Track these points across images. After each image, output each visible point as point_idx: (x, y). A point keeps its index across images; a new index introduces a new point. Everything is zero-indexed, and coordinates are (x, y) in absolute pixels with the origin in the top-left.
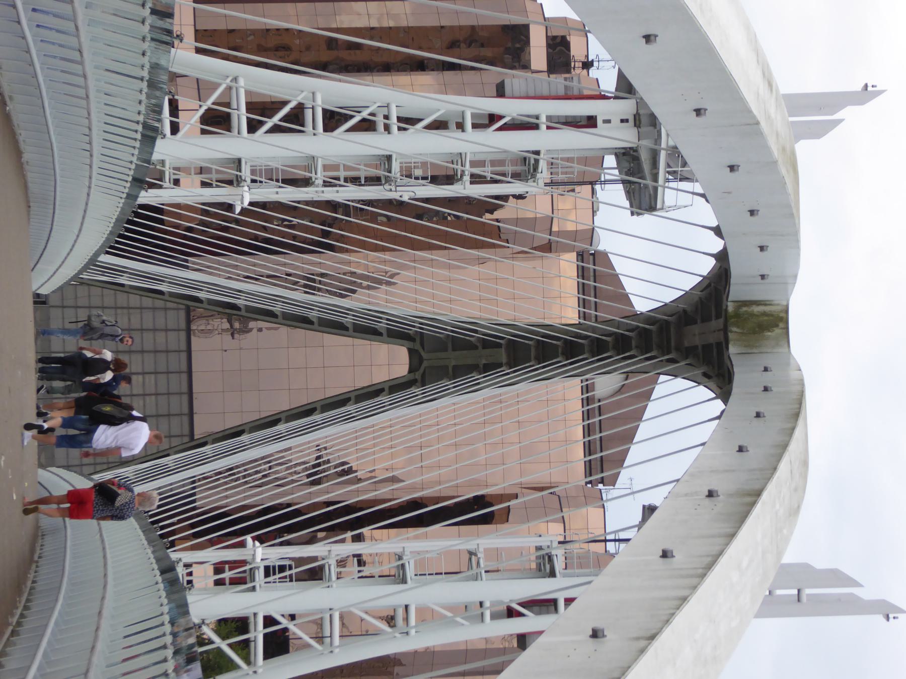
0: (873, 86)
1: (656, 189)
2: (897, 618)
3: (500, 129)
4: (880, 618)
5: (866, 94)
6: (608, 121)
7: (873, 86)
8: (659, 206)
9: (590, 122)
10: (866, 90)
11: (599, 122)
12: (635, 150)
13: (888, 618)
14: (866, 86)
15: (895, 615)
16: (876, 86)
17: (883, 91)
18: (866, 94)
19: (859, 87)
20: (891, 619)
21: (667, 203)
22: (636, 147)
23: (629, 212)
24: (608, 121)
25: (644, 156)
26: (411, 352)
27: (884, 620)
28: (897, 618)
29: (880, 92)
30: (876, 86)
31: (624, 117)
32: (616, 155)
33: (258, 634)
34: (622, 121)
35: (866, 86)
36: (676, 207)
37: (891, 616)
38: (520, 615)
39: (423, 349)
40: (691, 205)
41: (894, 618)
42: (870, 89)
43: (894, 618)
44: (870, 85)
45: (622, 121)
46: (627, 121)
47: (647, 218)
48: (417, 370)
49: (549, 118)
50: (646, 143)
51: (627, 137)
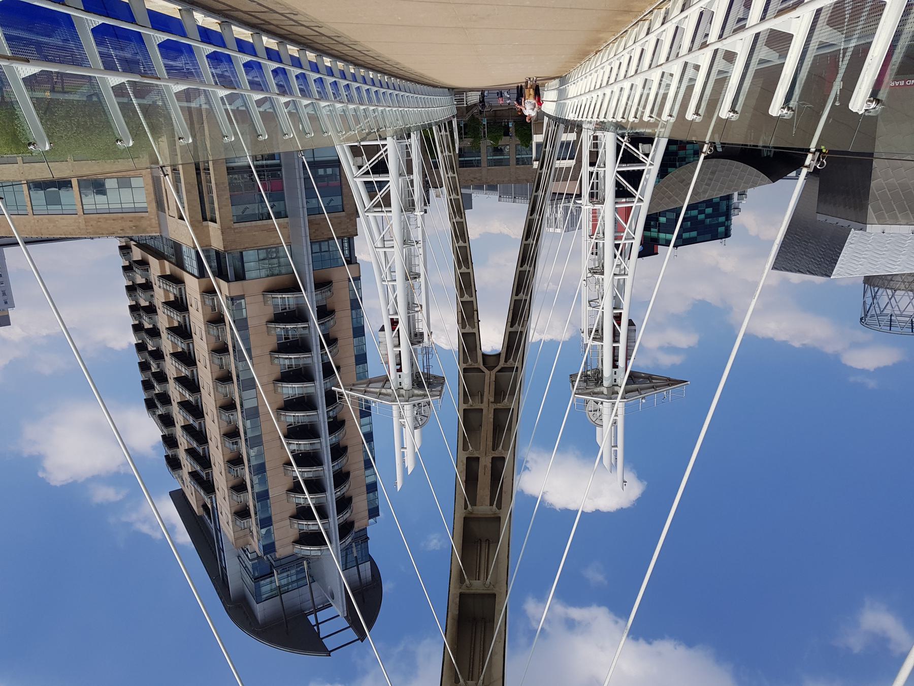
3: (614, 326)
6: (615, 374)
9: (615, 366)
11: (615, 370)
14: (626, 482)
24: (615, 374)
25: (598, 390)
38: (393, 330)
39: (499, 371)
42: (624, 483)
46: (615, 382)
48: (484, 364)
50: (605, 392)
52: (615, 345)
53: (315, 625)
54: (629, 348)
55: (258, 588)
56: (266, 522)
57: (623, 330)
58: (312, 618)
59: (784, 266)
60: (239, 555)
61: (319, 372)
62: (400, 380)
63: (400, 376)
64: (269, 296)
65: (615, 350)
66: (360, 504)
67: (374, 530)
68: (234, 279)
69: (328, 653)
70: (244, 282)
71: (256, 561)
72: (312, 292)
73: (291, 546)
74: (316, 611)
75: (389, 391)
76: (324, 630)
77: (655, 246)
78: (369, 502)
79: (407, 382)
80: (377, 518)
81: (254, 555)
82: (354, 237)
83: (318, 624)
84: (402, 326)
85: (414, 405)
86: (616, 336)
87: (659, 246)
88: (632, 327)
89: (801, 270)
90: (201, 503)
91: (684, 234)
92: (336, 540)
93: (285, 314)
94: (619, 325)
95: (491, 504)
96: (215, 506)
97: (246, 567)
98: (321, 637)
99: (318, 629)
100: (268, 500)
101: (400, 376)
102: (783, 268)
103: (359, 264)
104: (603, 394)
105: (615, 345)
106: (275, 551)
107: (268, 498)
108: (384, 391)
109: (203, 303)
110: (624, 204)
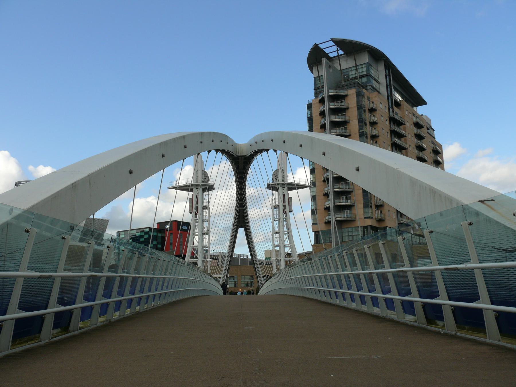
1: (209, 185)
3: (198, 212)
8: (213, 185)
12: (202, 189)
23: (213, 190)
26: (240, 227)
32: (203, 193)
33: (288, 259)
36: (213, 182)
38: (286, 212)
47: (215, 186)
49: (196, 204)
51: (200, 190)
52: (197, 205)
53: (339, 50)
54: (192, 203)
55: (368, 70)
56: (360, 107)
57: (194, 210)
58: (341, 52)
59: (104, 222)
60: (379, 84)
61: (330, 182)
62: (284, 191)
64: (353, 218)
65: (197, 203)
66: (316, 112)
67: (310, 96)
68: (368, 226)
69: (332, 40)
70: (364, 225)
71: (368, 85)
72: (332, 220)
73: (349, 94)
74: (339, 56)
76: (335, 48)
77: (158, 228)
78: (311, 111)
79: (280, 189)
80: (308, 103)
81: (368, 88)
82: (314, 244)
83: (337, 51)
85: (278, 180)
86: (197, 208)
87: (156, 228)
88: (191, 212)
89: (97, 220)
90: (402, 107)
91: (144, 234)
92: (326, 97)
93: (346, 209)
95: (239, 210)
96: (391, 110)
97: (375, 80)
98: (336, 46)
99: (337, 48)
100: (358, 118)
101: (284, 193)
102: (104, 221)
103: (312, 231)
105: (197, 205)
106: (356, 92)
107: (358, 119)
108: (291, 187)
109: (384, 214)
110: (194, 260)
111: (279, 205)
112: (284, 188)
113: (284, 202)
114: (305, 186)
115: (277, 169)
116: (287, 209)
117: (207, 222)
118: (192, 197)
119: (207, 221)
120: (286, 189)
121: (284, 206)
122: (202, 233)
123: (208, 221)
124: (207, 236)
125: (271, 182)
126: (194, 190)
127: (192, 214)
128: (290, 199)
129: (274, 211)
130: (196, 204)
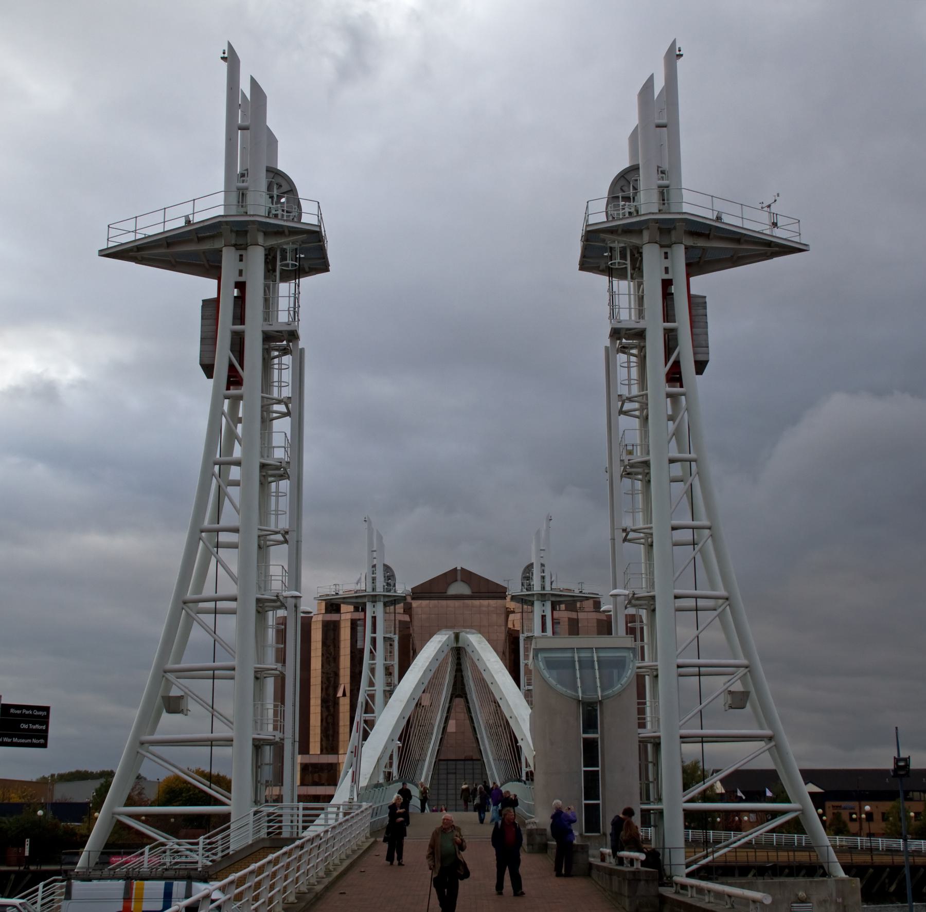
0: (224, 53)
2: (679, 48)
3: (242, 364)
4: (680, 62)
5: (231, 58)
7: (224, 53)
8: (317, 229)
10: (226, 58)
13: (681, 55)
15: (677, 50)
16: (224, 50)
17: (230, 46)
18: (231, 58)
19: (224, 65)
20: (681, 53)
21: (316, 223)
22: (265, 250)
27: (682, 59)
28: (679, 48)
29: (230, 46)
30: (224, 50)
31: (238, 258)
34: (241, 260)
35: (223, 58)
37: (678, 53)
38: (677, 364)
40: (318, 203)
41: (680, 51)
42: (226, 55)
43: (680, 51)
44: (223, 55)
45: (241, 260)
46: (241, 256)
50: (261, 239)
52: (239, 327)
57: (223, 356)
62: (667, 263)
63: (667, 270)
65: (240, 317)
75: (690, 242)
79: (651, 256)
84: (658, 367)
86: (238, 344)
88: (207, 362)
94: (232, 367)
104: (266, 234)
111: (640, 334)
112: (666, 250)
113: (668, 314)
114: (769, 244)
115: (626, 164)
116: (686, 352)
117: (288, 418)
118: (216, 296)
119: (288, 414)
120: (679, 255)
121: (671, 341)
122: (263, 466)
123: (295, 413)
124: (284, 485)
125: (599, 217)
126: (229, 258)
127: (211, 381)
128: (697, 305)
129: (618, 367)
130: (234, 324)
